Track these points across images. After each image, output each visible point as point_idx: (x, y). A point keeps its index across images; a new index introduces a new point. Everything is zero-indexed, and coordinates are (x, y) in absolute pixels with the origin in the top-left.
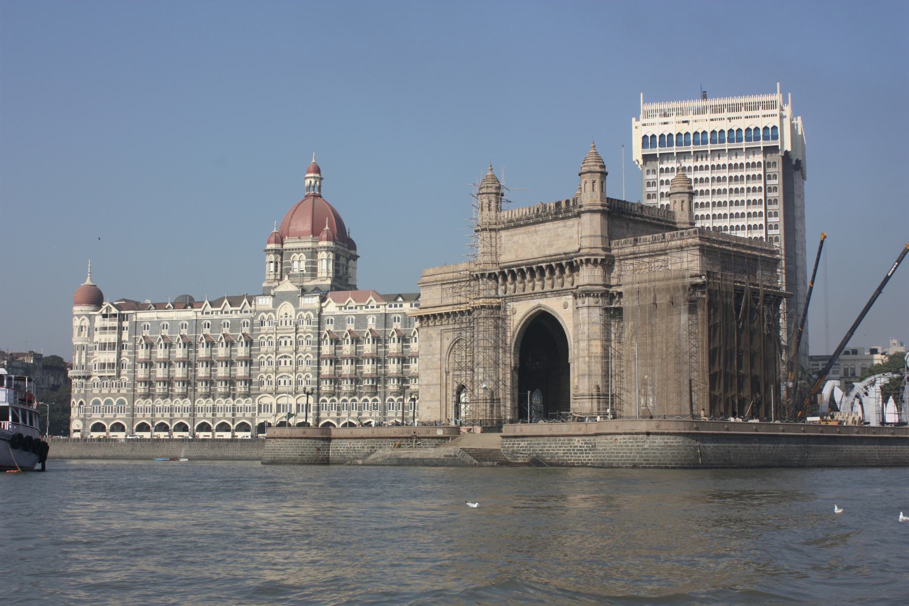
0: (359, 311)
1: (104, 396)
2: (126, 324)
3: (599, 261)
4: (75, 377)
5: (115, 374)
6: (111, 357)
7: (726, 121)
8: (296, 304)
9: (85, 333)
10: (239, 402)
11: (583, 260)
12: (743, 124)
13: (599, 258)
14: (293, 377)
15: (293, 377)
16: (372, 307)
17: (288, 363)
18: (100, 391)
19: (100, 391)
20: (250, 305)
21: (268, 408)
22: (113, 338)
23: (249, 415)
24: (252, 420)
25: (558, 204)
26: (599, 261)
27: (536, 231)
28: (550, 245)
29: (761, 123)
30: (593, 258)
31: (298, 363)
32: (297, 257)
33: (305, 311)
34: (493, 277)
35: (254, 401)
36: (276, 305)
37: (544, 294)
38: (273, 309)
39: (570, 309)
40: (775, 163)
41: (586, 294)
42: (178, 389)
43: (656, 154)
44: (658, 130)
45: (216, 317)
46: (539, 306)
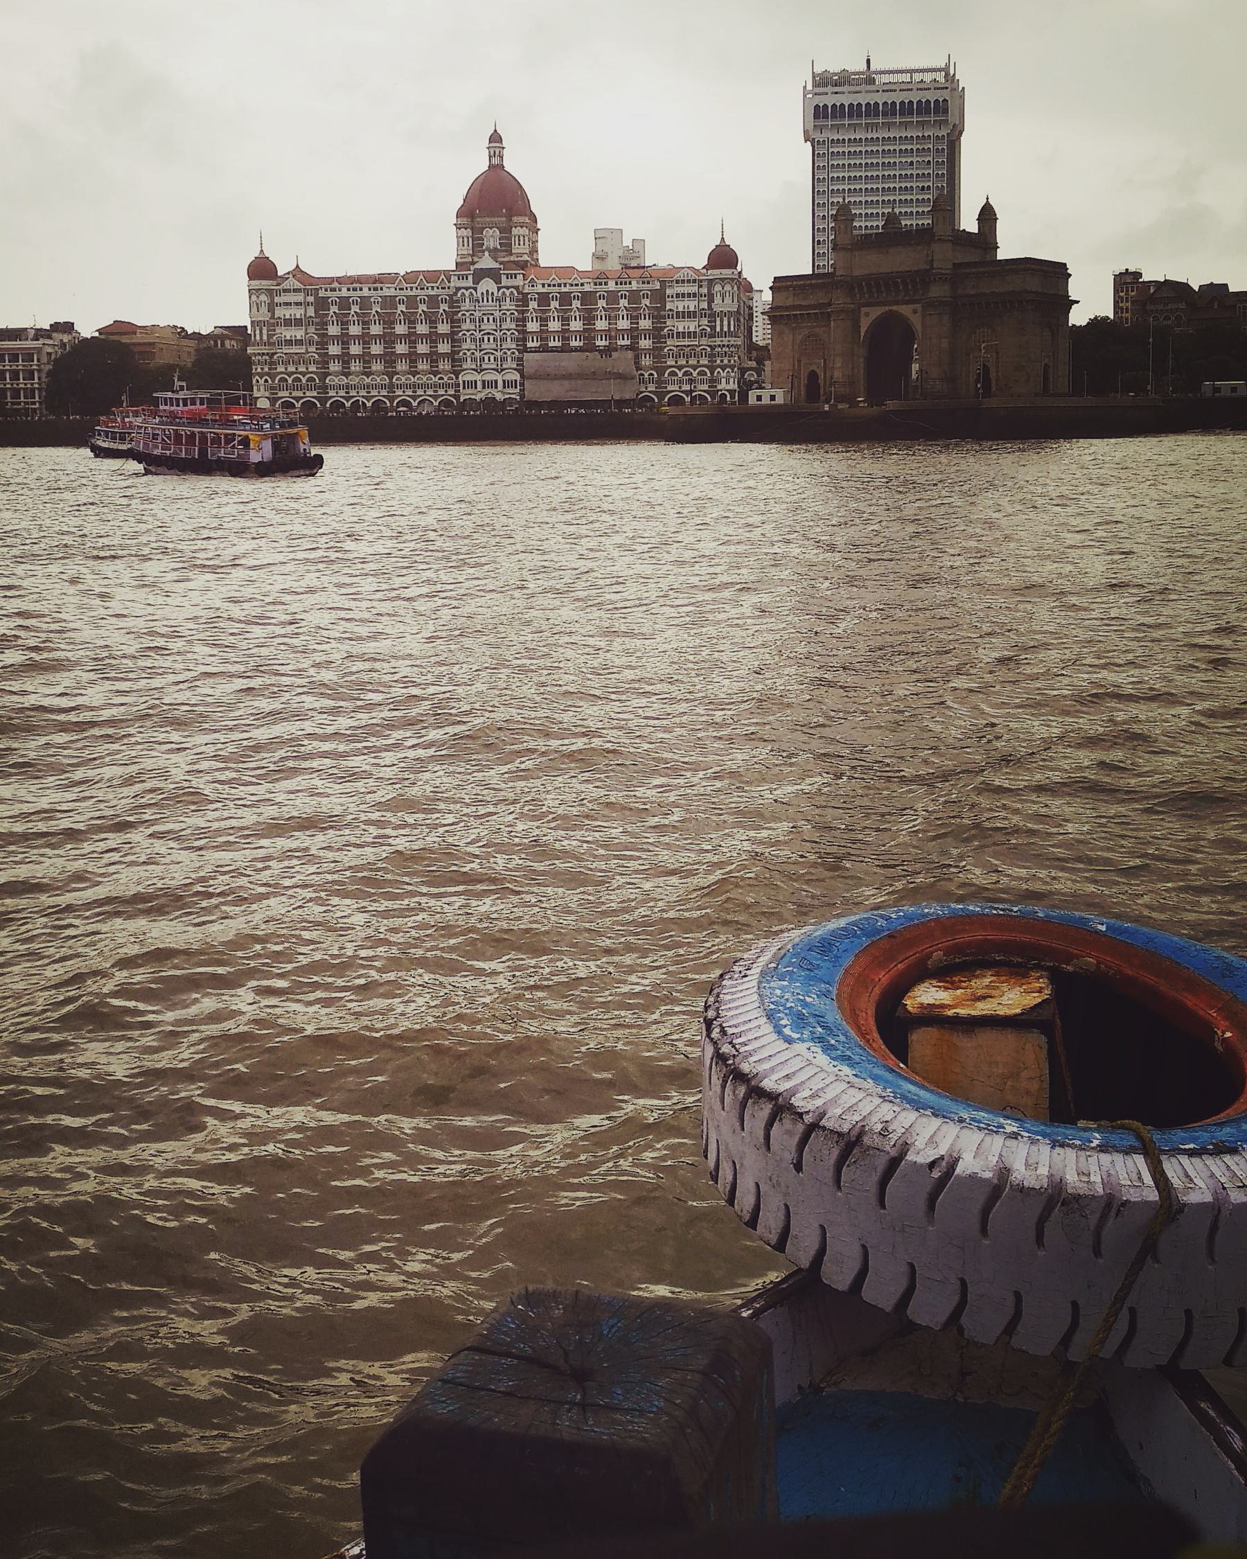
0: (564, 289)
1: (290, 374)
2: (311, 299)
4: (255, 355)
5: (303, 351)
6: (299, 333)
8: (498, 281)
9: (264, 309)
10: (440, 379)
14: (498, 354)
15: (498, 354)
16: (577, 285)
17: (492, 338)
18: (286, 369)
19: (286, 369)
20: (449, 282)
21: (474, 384)
22: (298, 313)
23: (451, 392)
24: (457, 397)
29: (931, 96)
31: (503, 340)
32: (491, 231)
33: (508, 288)
35: (457, 378)
36: (476, 282)
38: (471, 284)
39: (919, 314)
42: (377, 367)
44: (830, 100)
45: (412, 294)
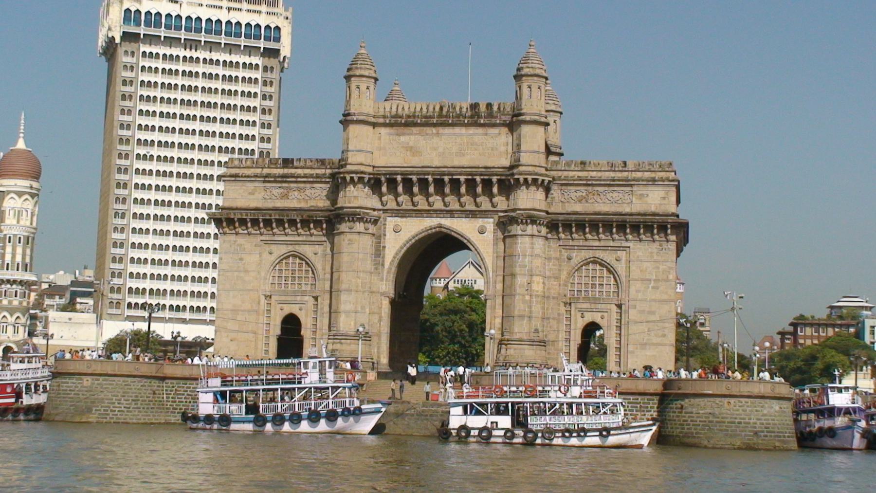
3: (546, 183)
7: (225, 11)
11: (530, 178)
12: (244, 18)
13: (547, 179)
25: (474, 106)
26: (546, 183)
27: (438, 134)
28: (460, 153)
30: (541, 178)
34: (372, 182)
37: (451, 213)
39: (489, 235)
40: (272, 68)
41: (531, 220)
43: (139, 34)
46: (440, 226)
